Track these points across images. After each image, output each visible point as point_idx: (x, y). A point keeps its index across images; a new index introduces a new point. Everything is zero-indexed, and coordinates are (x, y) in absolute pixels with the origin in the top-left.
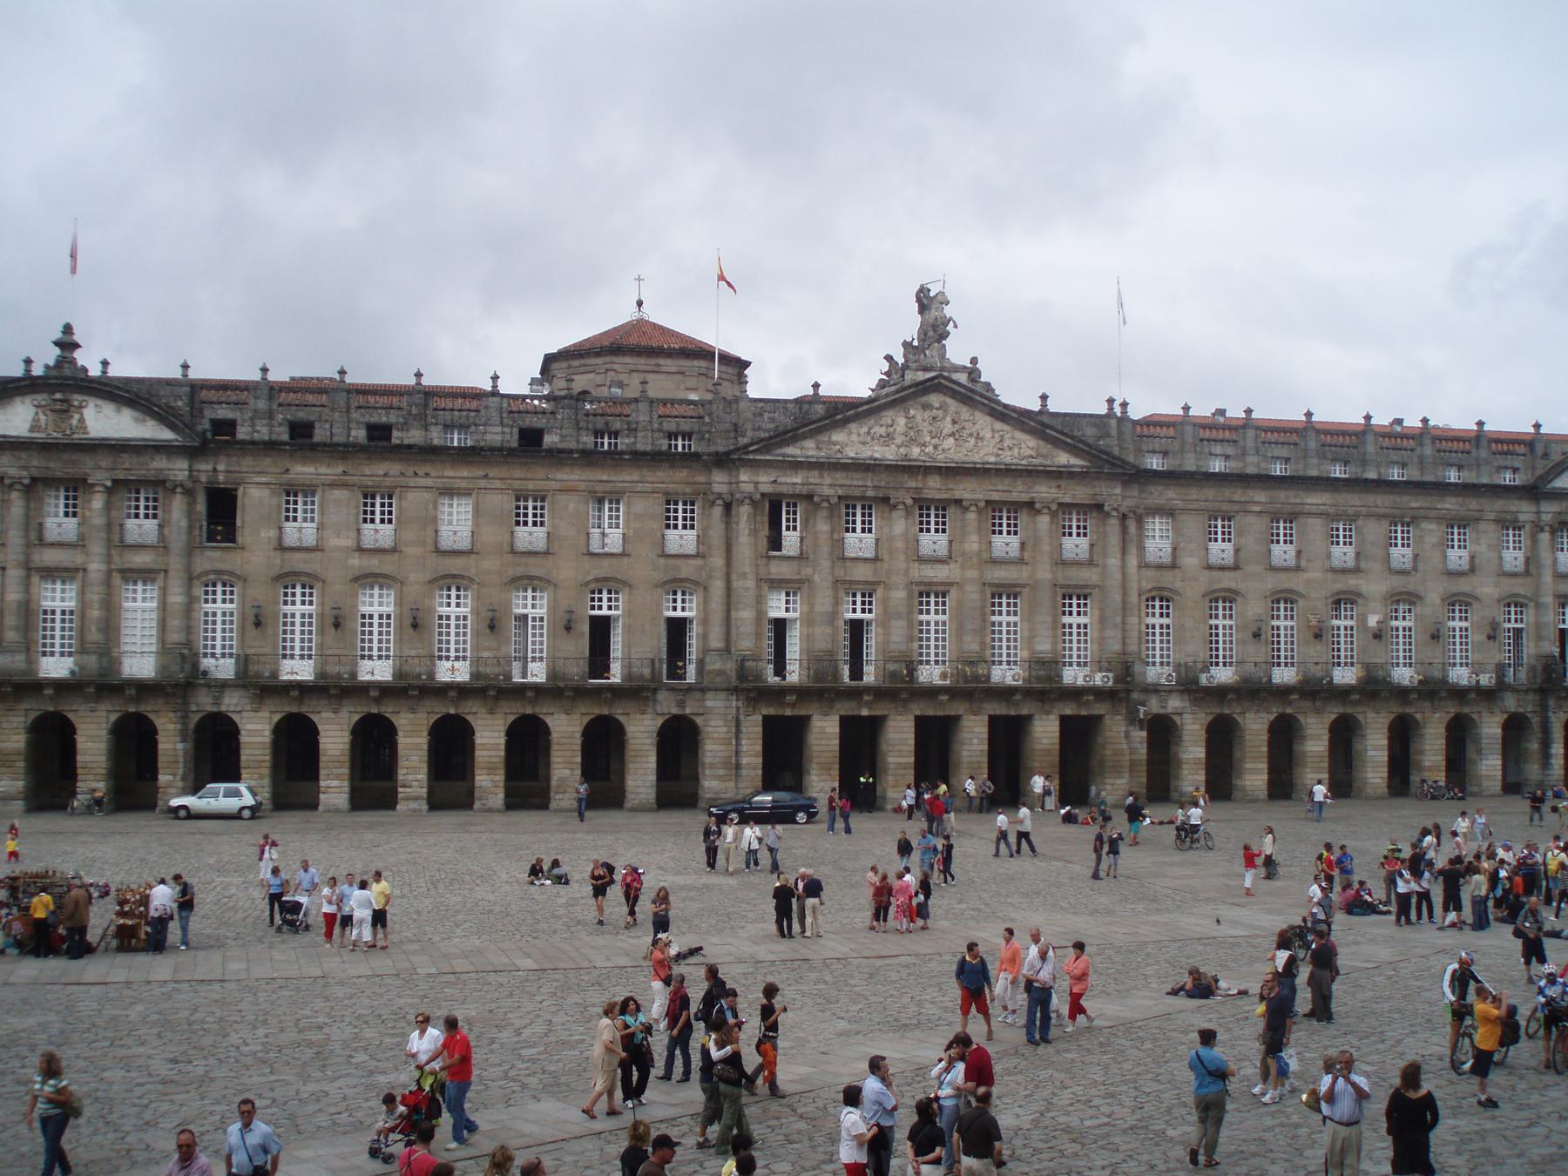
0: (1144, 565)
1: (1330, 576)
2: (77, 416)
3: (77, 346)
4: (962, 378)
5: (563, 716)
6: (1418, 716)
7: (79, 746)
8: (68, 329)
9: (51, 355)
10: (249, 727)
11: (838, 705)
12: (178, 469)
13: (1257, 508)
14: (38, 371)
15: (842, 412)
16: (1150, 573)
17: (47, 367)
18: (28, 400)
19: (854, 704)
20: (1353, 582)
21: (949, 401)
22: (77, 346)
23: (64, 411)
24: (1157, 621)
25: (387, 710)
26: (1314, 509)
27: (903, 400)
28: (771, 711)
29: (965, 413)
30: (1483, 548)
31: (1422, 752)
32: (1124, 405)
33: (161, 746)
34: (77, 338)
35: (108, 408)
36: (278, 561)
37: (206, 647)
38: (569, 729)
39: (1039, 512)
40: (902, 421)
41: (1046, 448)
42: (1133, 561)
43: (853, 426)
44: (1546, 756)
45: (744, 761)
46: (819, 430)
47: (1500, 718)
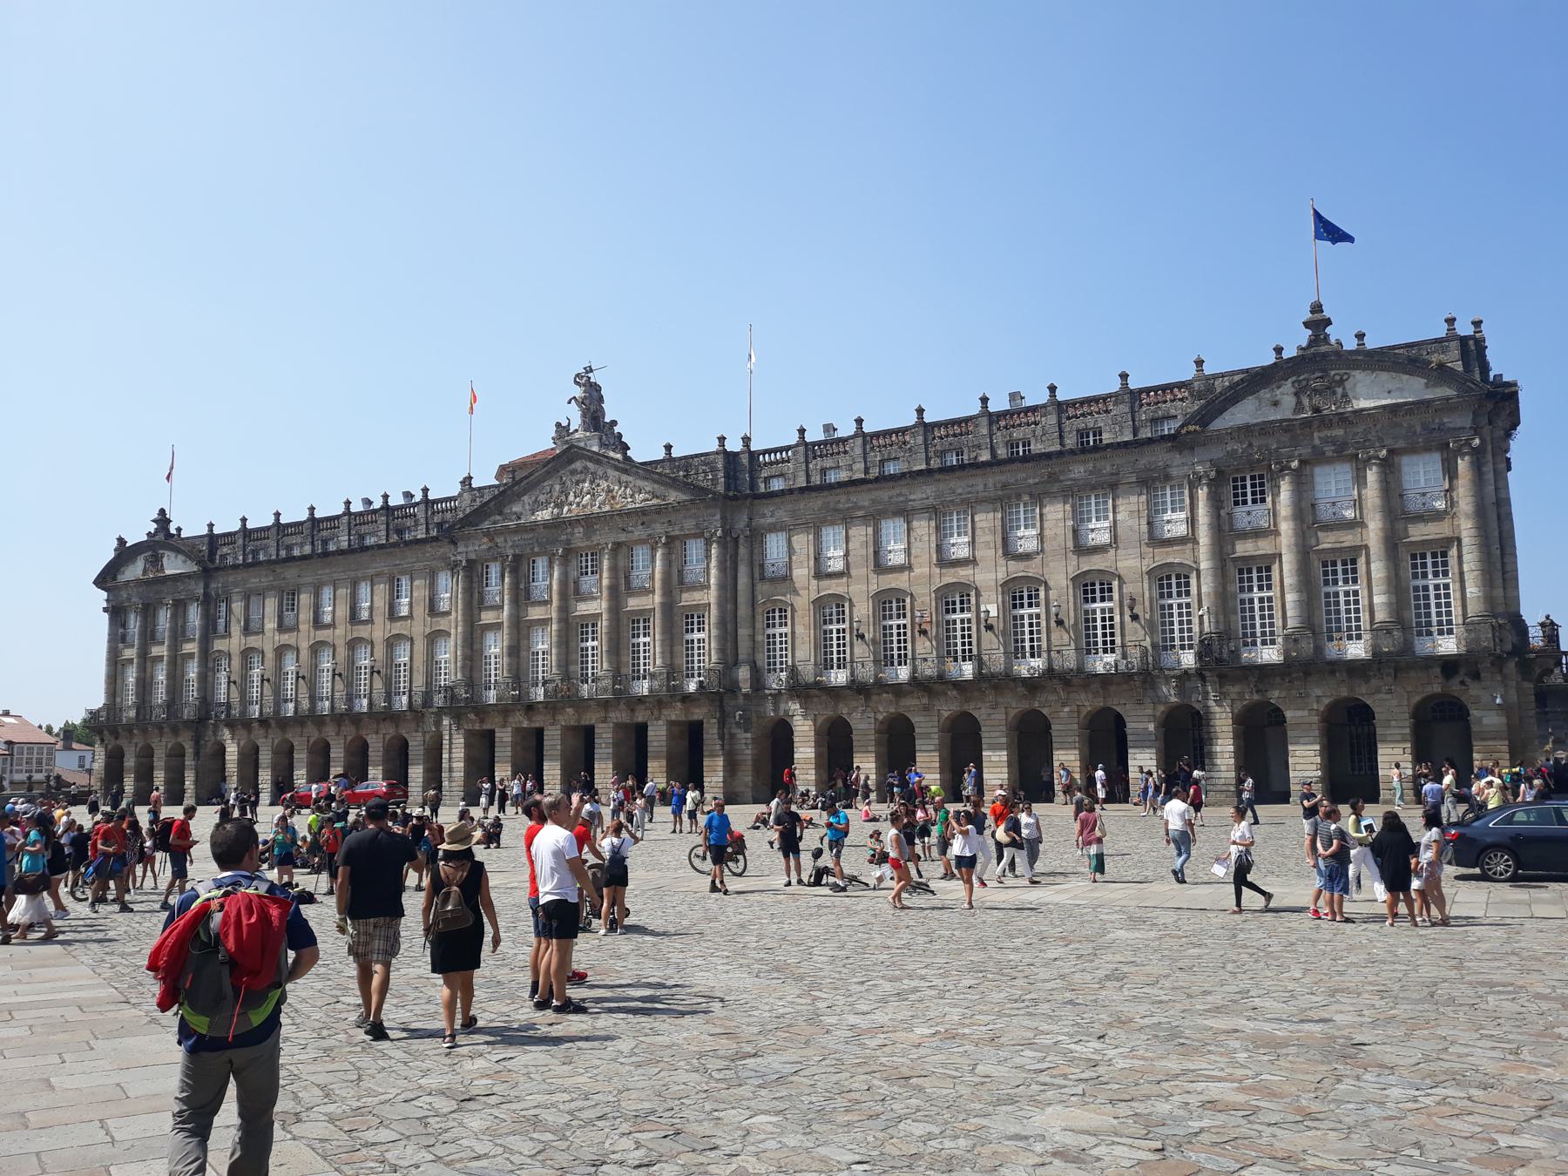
6: (1045, 711)
8: (162, 511)
11: (511, 719)
13: (860, 513)
20: (963, 574)
21: (590, 465)
23: (156, 561)
26: (917, 504)
40: (557, 487)
42: (743, 580)
43: (525, 498)
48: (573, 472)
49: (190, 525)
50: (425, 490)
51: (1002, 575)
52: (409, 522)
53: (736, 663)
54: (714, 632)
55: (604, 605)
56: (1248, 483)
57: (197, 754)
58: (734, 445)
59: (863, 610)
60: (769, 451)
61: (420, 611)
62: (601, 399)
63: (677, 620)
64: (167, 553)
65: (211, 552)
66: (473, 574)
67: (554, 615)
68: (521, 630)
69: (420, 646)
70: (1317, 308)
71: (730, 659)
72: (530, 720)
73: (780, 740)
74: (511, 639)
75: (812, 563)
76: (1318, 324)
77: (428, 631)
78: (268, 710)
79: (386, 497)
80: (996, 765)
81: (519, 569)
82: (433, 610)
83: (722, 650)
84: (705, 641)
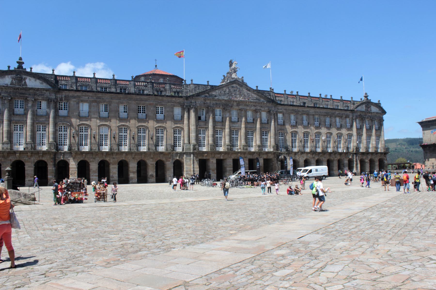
0: (278, 124)
2: (24, 82)
3: (23, 63)
4: (241, 81)
5: (151, 160)
7: (26, 169)
8: (21, 59)
9: (16, 65)
10: (72, 163)
11: (216, 156)
14: (12, 68)
15: (214, 88)
16: (279, 127)
17: (15, 68)
18: (10, 76)
19: (219, 156)
21: (238, 86)
22: (23, 63)
24: (281, 138)
25: (107, 159)
27: (228, 85)
28: (201, 158)
29: (241, 88)
30: (343, 123)
31: (333, 167)
32: (273, 89)
33: (49, 168)
34: (23, 61)
35: (33, 80)
37: (59, 143)
38: (153, 163)
39: (257, 112)
40: (228, 90)
43: (217, 91)
44: (357, 167)
45: (195, 169)
46: (210, 91)
47: (347, 159)
48: (232, 87)
56: (19, 102)
57: (55, 165)
60: (278, 94)
64: (28, 78)
70: (366, 94)
76: (366, 97)
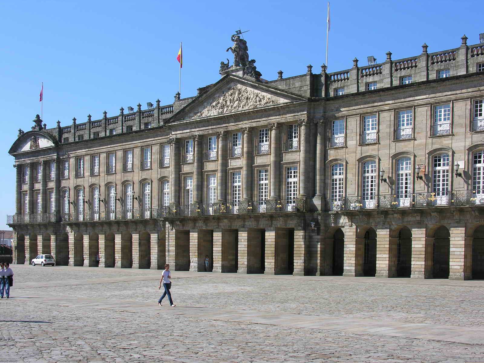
1: (430, 140)
8: (38, 116)
11: (197, 225)
12: (55, 156)
13: (387, 108)
20: (446, 142)
23: (36, 141)
26: (421, 102)
35: (43, 139)
36: (75, 182)
41: (274, 98)
45: (170, 249)
49: (50, 124)
50: (158, 101)
51: (468, 144)
52: (150, 119)
53: (314, 195)
54: (302, 178)
55: (245, 162)
58: (317, 71)
59: (386, 164)
61: (155, 166)
62: (246, 48)
63: (281, 171)
65: (59, 136)
66: (180, 146)
67: (219, 168)
68: (203, 178)
69: (155, 184)
71: (310, 192)
72: (206, 225)
73: (337, 240)
74: (198, 181)
75: (358, 137)
77: (159, 177)
78: (88, 217)
79: (140, 106)
80: (383, 259)
81: (203, 143)
82: (161, 165)
83: (306, 188)
84: (296, 181)
